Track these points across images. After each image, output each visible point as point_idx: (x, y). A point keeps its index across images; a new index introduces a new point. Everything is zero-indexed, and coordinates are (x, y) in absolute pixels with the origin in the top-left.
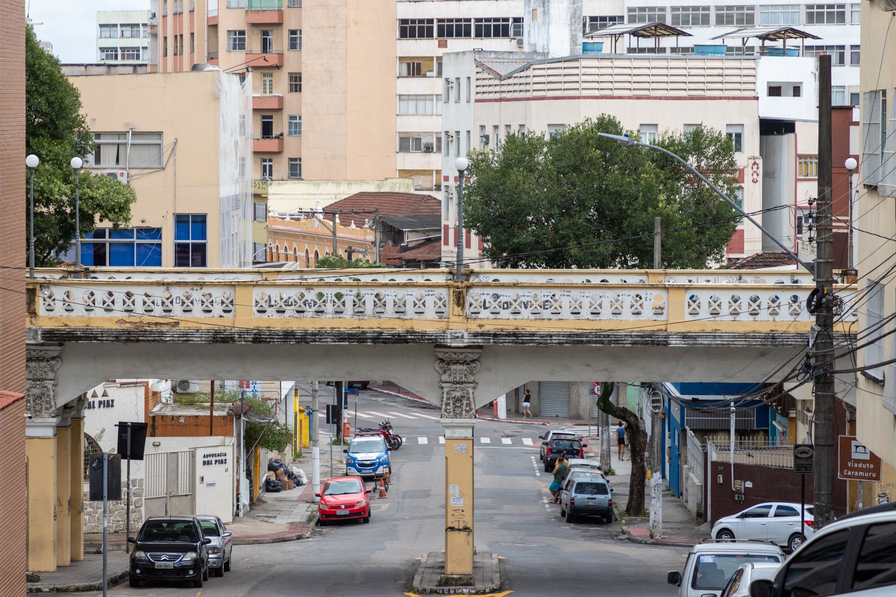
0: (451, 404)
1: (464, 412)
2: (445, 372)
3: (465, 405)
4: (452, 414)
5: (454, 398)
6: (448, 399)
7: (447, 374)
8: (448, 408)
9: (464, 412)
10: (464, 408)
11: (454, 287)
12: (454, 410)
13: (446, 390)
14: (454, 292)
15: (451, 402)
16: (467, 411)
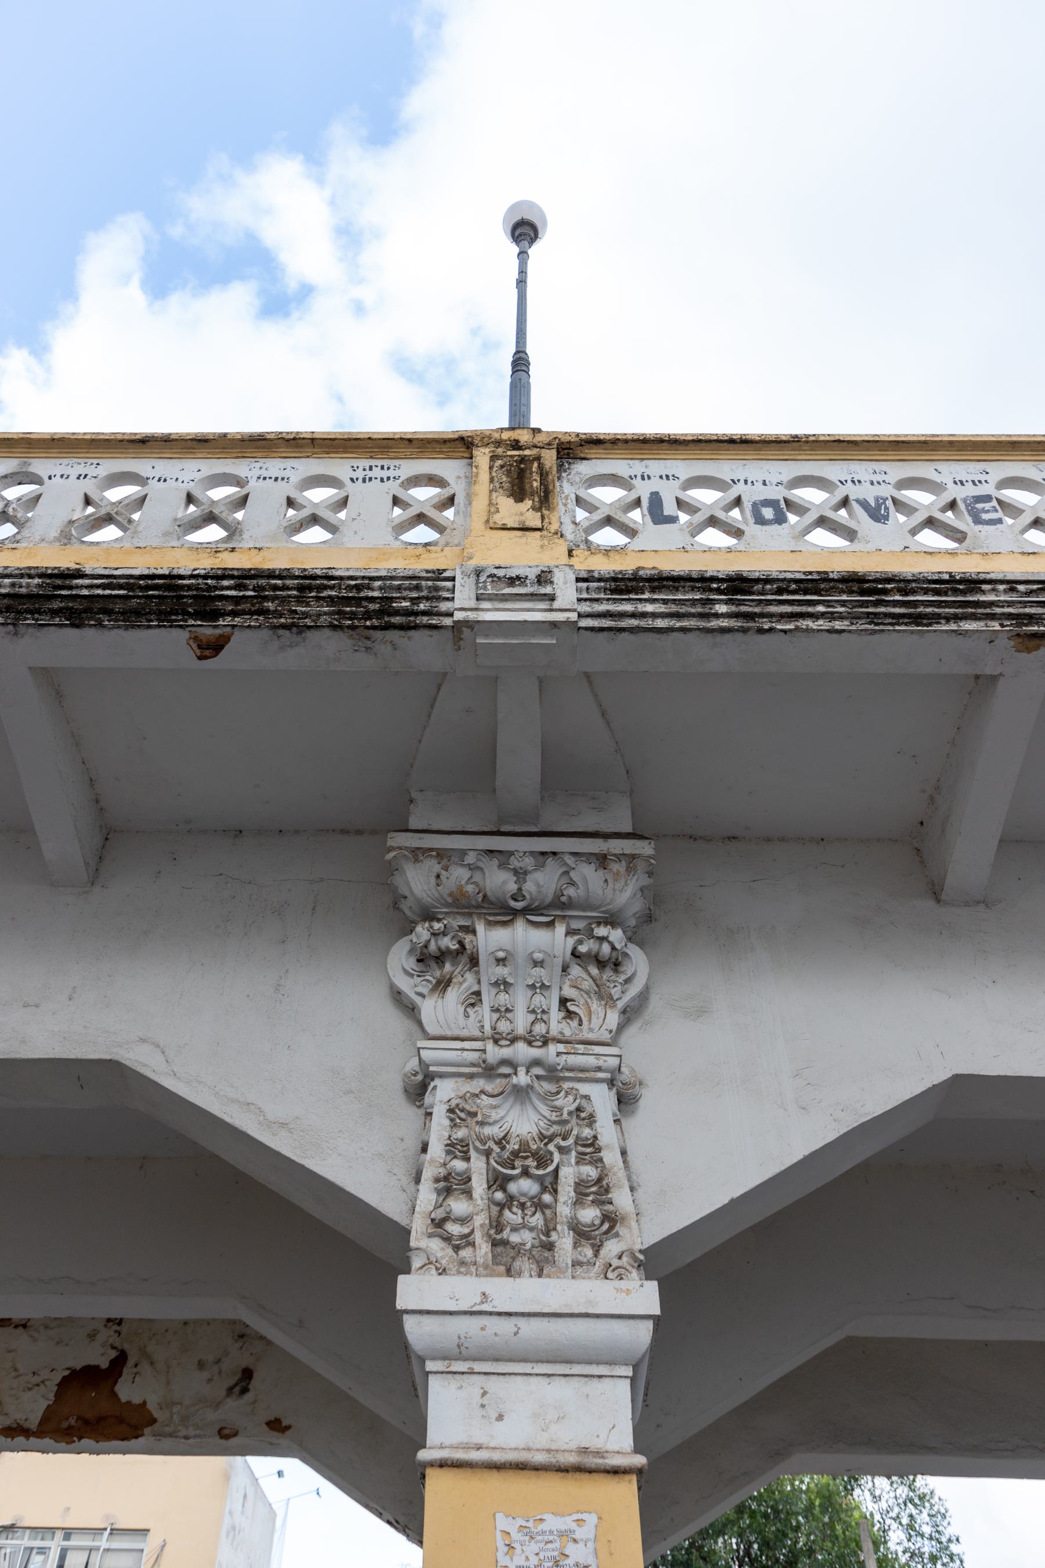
0: (479, 1185)
1: (564, 1241)
2: (442, 985)
3: (567, 1191)
4: (484, 1248)
5: (502, 1142)
6: (458, 1149)
7: (453, 995)
8: (458, 1206)
9: (564, 1241)
10: (564, 1210)
11: (498, 443)
12: (498, 1225)
13: (444, 1092)
14: (494, 458)
15: (478, 1168)
16: (581, 1233)
